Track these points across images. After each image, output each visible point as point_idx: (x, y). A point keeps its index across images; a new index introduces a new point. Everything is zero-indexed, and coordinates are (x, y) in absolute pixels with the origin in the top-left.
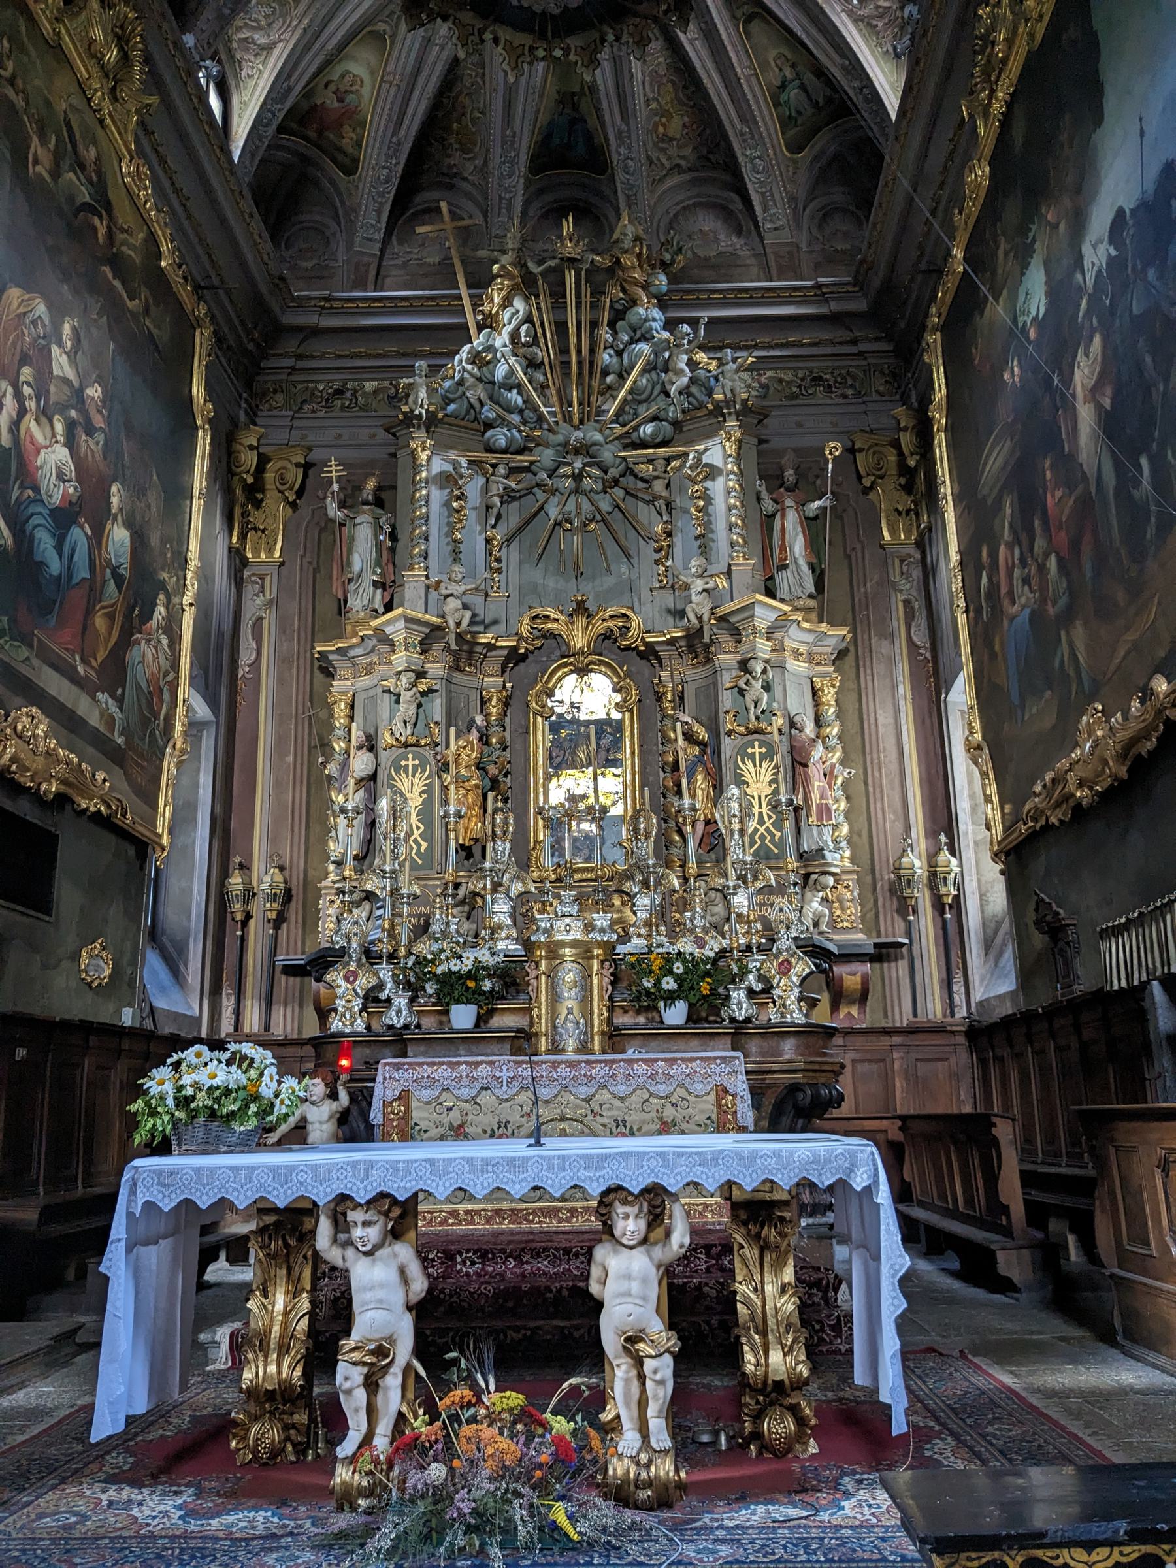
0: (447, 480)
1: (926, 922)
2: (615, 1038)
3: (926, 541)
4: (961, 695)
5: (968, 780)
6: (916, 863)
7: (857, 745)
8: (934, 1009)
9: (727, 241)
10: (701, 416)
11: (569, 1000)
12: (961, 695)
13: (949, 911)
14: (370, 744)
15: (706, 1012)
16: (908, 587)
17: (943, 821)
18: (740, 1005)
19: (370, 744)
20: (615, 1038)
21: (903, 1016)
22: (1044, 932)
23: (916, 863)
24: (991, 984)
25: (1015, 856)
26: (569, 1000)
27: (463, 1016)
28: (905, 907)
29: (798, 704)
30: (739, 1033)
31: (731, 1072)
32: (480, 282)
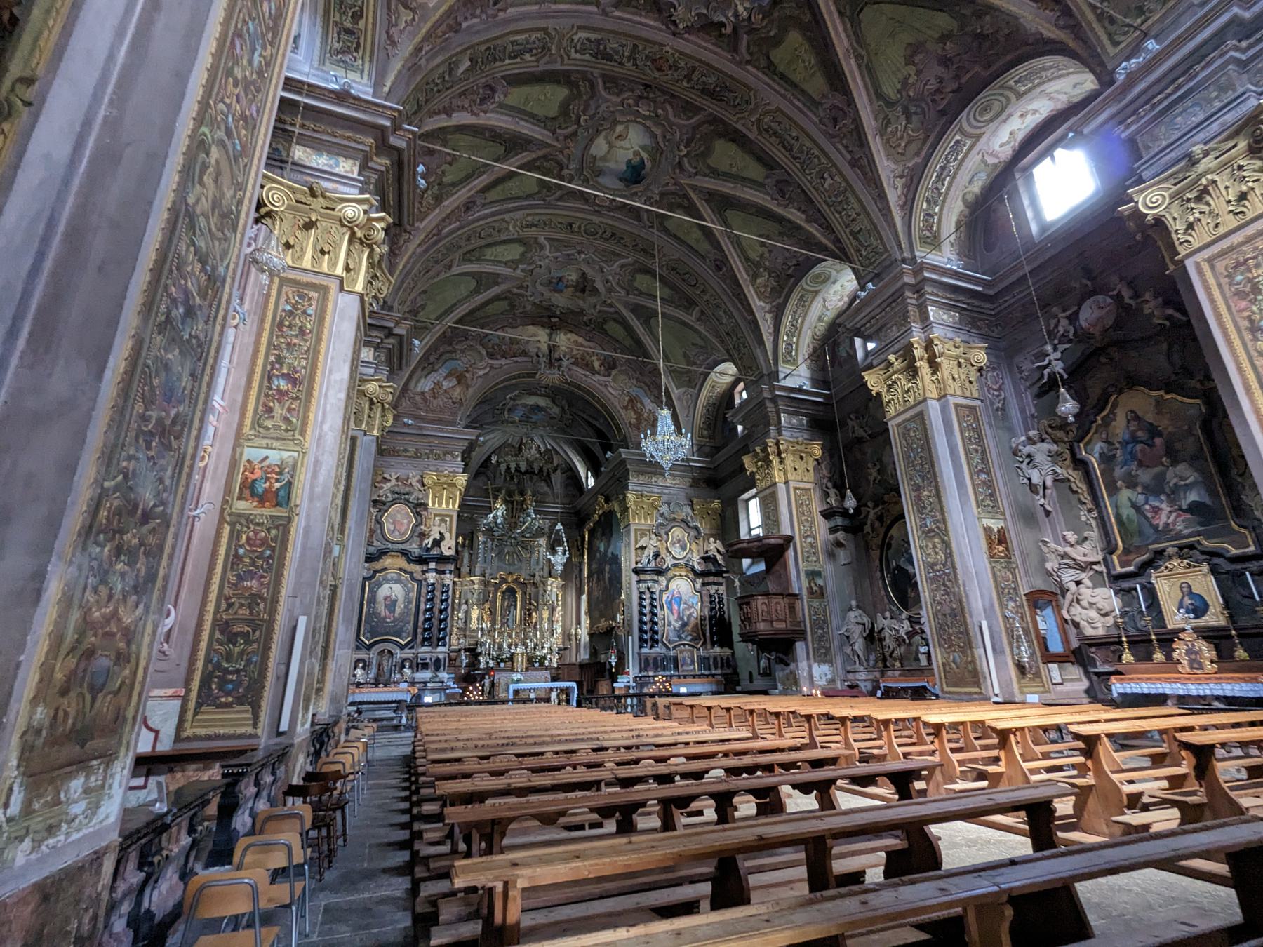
0: (484, 543)
1: (573, 642)
2: (527, 669)
3: (581, 563)
4: (584, 597)
5: (585, 621)
6: (573, 631)
7: (564, 605)
8: (573, 660)
9: (546, 489)
10: (539, 533)
11: (520, 662)
12: (584, 597)
13: (578, 641)
14: (466, 603)
15: (542, 664)
16: (576, 572)
17: (579, 622)
18: (547, 663)
19: (466, 603)
20: (527, 669)
21: (567, 662)
22: (594, 652)
23: (573, 631)
24: (585, 656)
25: (591, 635)
26: (520, 662)
27: (502, 665)
28: (570, 640)
29: (554, 598)
30: (547, 668)
31: (548, 675)
32: (496, 498)
